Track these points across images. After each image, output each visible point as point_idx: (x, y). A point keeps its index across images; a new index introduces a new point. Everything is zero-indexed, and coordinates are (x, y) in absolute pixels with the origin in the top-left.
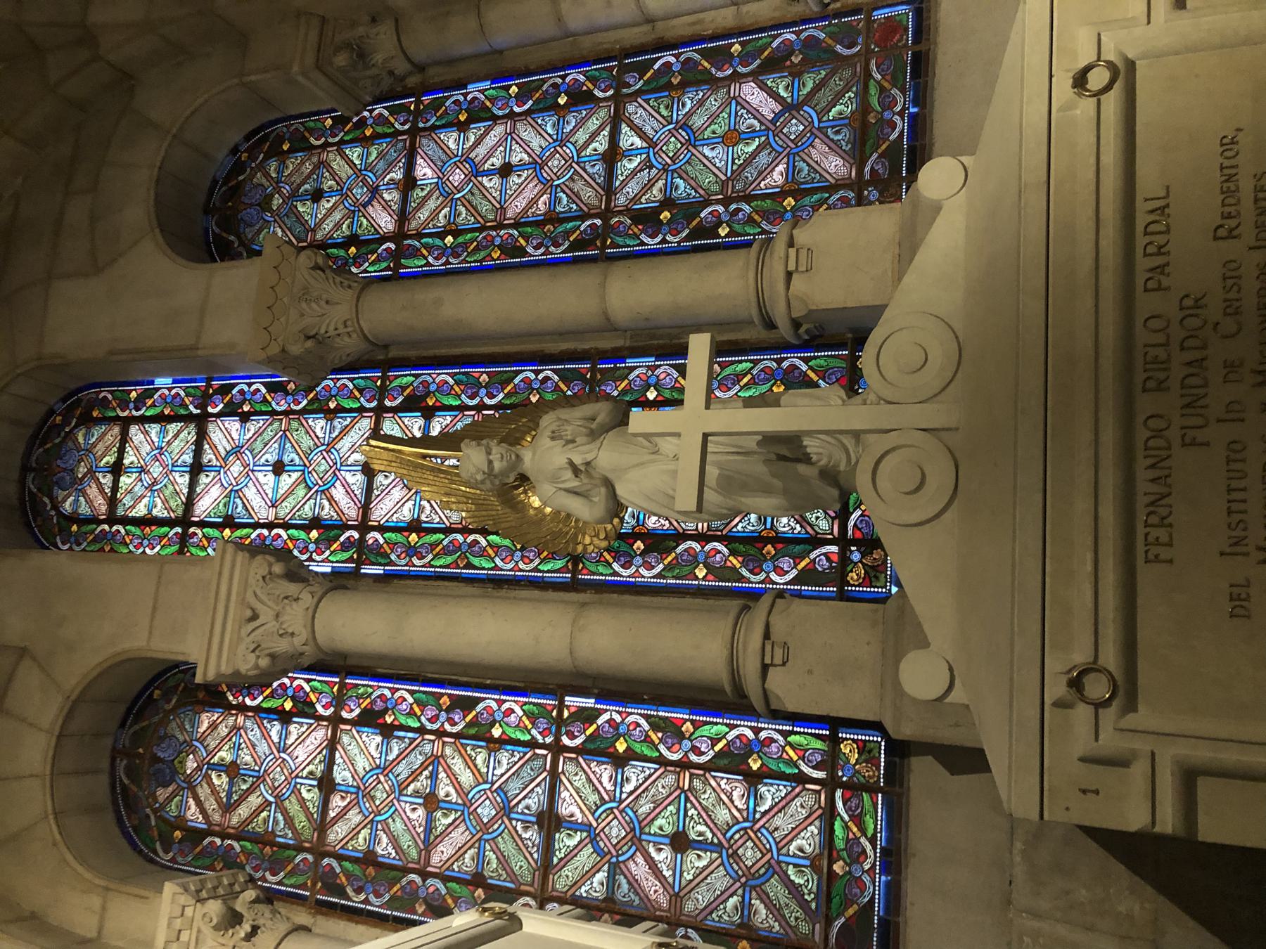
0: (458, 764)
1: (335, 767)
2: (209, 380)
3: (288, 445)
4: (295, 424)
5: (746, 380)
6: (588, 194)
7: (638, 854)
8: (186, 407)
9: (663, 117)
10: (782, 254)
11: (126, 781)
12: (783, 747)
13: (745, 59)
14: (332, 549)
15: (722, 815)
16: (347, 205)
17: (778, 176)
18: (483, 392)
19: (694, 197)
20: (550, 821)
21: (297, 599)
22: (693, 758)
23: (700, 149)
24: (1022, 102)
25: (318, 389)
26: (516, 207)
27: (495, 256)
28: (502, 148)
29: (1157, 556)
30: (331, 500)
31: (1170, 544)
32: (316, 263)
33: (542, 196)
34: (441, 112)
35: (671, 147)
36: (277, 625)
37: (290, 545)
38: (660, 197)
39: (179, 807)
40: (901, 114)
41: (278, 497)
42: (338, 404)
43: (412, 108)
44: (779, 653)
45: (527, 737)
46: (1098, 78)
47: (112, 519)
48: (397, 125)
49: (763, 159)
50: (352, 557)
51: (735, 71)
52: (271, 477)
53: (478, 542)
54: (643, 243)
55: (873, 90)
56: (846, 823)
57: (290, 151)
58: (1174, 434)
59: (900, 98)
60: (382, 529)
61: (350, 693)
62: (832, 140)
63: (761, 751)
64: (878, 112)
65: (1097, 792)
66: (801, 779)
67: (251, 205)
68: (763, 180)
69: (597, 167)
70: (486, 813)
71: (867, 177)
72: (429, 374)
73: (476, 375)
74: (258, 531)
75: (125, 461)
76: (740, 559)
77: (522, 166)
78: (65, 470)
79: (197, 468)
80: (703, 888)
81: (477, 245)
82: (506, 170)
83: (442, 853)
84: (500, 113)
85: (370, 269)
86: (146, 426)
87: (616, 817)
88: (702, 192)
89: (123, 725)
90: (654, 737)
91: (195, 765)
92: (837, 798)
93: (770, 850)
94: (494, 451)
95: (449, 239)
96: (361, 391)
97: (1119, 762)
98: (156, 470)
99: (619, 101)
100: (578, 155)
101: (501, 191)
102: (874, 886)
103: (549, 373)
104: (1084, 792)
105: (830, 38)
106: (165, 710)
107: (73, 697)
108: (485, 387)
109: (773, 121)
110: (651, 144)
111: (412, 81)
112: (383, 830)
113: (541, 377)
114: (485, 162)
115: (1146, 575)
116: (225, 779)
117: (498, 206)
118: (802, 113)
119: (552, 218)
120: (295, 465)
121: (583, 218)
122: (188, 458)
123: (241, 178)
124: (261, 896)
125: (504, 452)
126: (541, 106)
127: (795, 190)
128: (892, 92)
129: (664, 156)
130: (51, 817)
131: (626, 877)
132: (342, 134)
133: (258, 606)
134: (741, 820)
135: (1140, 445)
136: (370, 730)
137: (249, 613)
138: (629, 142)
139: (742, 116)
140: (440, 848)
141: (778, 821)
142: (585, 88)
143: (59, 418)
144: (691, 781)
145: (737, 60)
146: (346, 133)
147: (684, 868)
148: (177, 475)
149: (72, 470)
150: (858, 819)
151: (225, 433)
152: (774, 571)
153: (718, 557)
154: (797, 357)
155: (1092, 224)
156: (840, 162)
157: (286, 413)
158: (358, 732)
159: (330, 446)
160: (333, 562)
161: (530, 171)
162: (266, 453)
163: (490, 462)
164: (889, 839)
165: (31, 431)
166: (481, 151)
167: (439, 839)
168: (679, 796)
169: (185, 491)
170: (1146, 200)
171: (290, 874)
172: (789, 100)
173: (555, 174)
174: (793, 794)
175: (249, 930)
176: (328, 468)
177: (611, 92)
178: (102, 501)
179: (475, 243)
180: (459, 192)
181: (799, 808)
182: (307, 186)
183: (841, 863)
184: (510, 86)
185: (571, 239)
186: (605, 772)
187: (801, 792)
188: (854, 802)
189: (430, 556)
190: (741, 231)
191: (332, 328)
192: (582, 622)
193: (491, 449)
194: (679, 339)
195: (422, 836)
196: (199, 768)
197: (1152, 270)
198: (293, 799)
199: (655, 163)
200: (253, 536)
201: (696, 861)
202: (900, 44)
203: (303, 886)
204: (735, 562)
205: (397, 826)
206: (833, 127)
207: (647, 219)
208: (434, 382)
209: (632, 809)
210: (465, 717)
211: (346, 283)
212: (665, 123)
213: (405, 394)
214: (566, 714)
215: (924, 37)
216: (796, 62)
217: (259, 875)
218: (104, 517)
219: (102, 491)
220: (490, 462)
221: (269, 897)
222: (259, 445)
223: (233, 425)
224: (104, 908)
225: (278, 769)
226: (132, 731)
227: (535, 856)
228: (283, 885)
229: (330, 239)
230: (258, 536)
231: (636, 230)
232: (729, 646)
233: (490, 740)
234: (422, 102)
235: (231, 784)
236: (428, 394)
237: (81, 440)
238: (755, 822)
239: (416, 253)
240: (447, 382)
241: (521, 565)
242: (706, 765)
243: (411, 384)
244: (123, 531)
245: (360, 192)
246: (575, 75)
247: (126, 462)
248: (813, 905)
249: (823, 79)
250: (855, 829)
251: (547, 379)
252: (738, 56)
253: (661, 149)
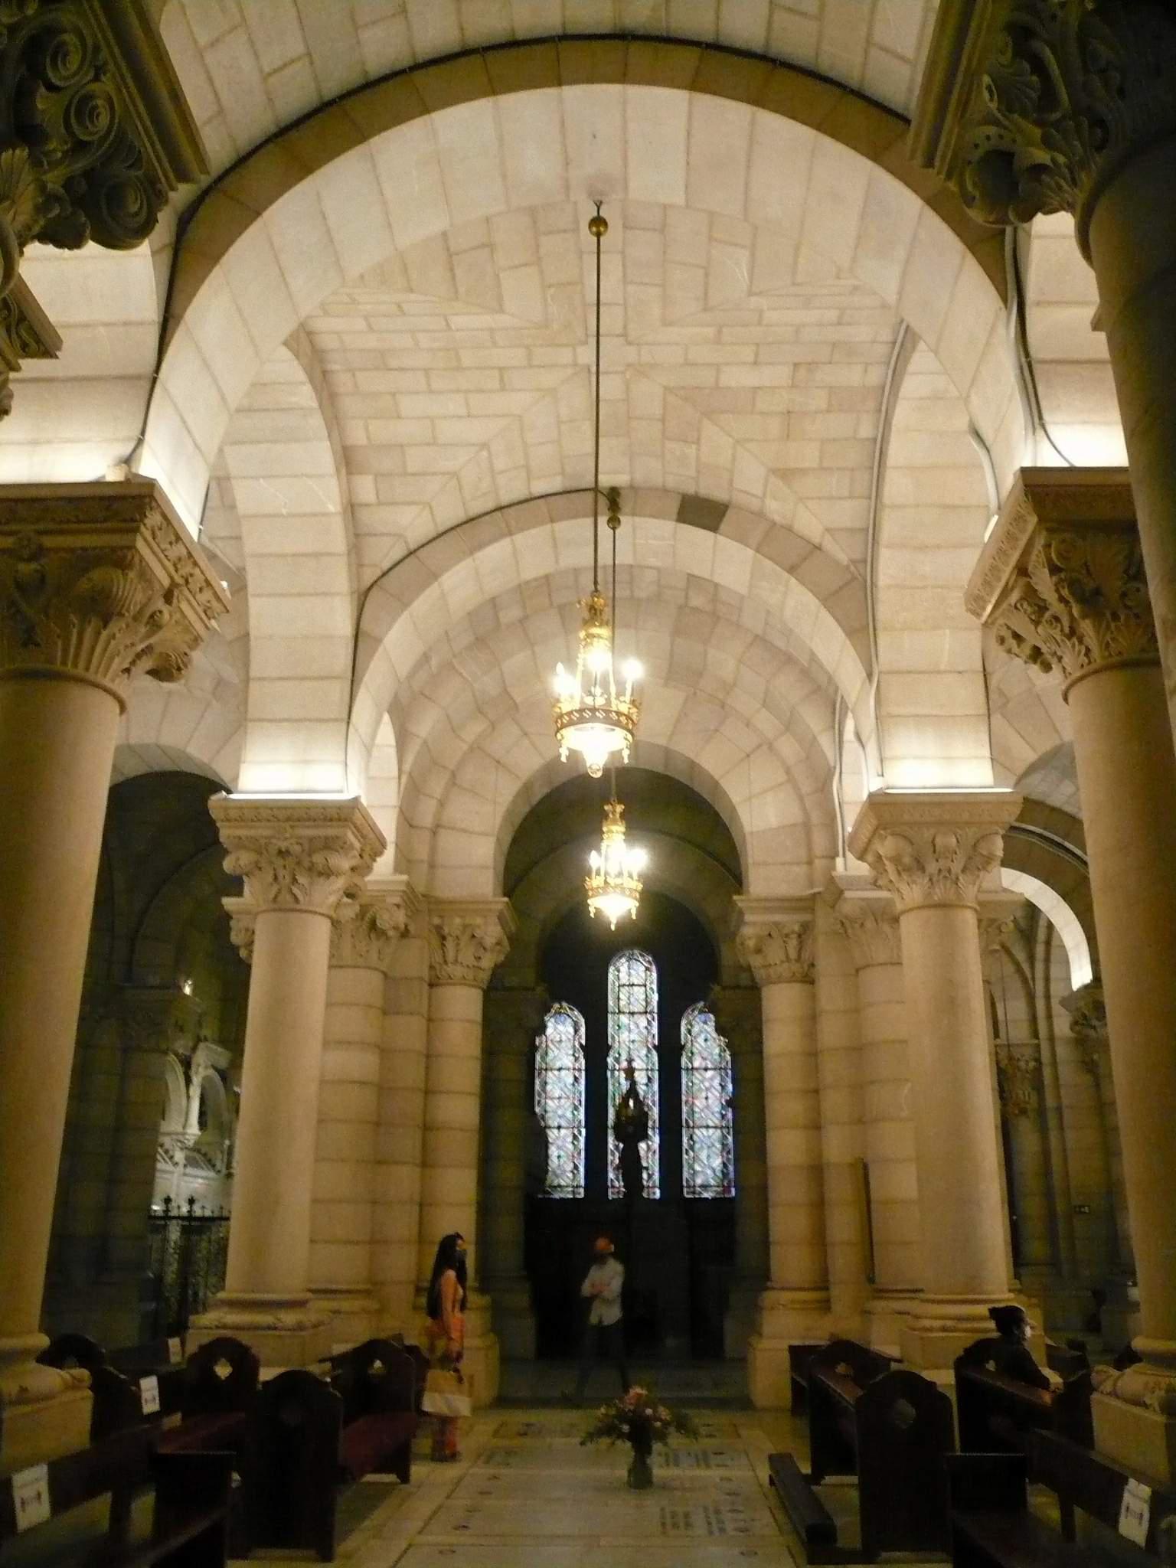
26: (697, 1102)
99: (722, 1128)
119: (693, 1112)
166: (713, 1090)
207: (691, 1138)
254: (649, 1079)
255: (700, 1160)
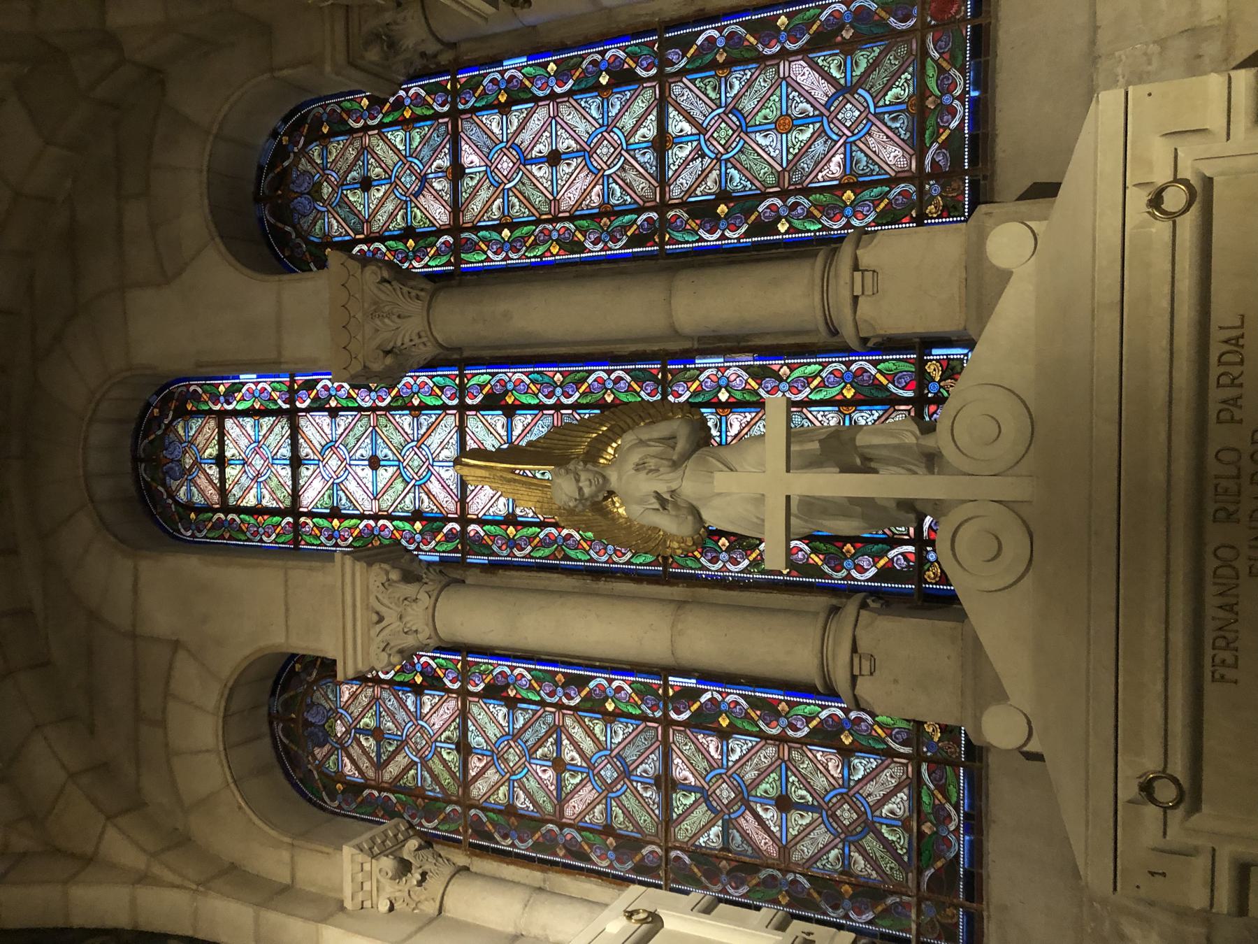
0: (578, 733)
1: (470, 734)
2: (292, 376)
3: (380, 441)
4: (383, 421)
5: (816, 382)
6: (641, 185)
7: (747, 812)
8: (275, 402)
9: (710, 99)
10: (848, 280)
11: (286, 741)
12: (872, 726)
13: (793, 34)
14: (437, 539)
15: (820, 782)
16: (398, 194)
17: (835, 167)
18: (559, 391)
19: (750, 190)
20: (666, 783)
21: (416, 600)
22: (790, 733)
23: (753, 136)
24: (1095, 214)
25: (399, 386)
26: (569, 198)
27: (555, 251)
28: (547, 134)
29: (1223, 661)
30: (429, 493)
31: (1235, 666)
32: (382, 277)
33: (594, 187)
34: (479, 91)
35: (723, 133)
36: (402, 625)
37: (397, 535)
38: (715, 189)
39: (336, 763)
40: (961, 98)
41: (379, 490)
42: (421, 401)
43: (449, 87)
44: (866, 665)
45: (638, 712)
46: (1175, 199)
47: (226, 509)
48: (435, 106)
49: (819, 147)
50: (457, 547)
51: (783, 48)
52: (368, 471)
53: (572, 536)
54: (701, 239)
55: (931, 71)
56: (932, 792)
57: (333, 134)
58: (1242, 565)
59: (960, 81)
60: (481, 522)
61: (473, 669)
62: (889, 128)
63: (851, 728)
64: (936, 97)
65: (1164, 874)
66: (890, 754)
67: (301, 194)
68: (821, 171)
69: (647, 156)
70: (609, 774)
71: (928, 169)
72: (505, 373)
73: (551, 374)
74: (365, 522)
75: (227, 454)
76: (821, 556)
77: (571, 154)
78: (172, 461)
79: (296, 462)
80: (807, 842)
81: (535, 239)
82: (554, 158)
83: (574, 808)
84: (540, 94)
85: (431, 263)
86: (241, 420)
87: (725, 781)
88: (758, 184)
89: (273, 694)
90: (753, 714)
91: (344, 729)
92: (923, 770)
93: (866, 813)
94: (583, 478)
95: (506, 233)
96: (442, 389)
97: (1188, 853)
98: (258, 463)
99: (663, 80)
100: (626, 142)
101: (552, 181)
102: (959, 844)
103: (621, 374)
104: (1153, 874)
105: (883, 9)
106: (308, 682)
107: (230, 684)
108: (560, 386)
109: (827, 106)
110: (702, 130)
111: (446, 58)
112: (520, 787)
113: (613, 376)
114: (532, 149)
115: (1212, 691)
116: (372, 741)
117: (551, 198)
118: (856, 96)
119: (607, 211)
120: (389, 460)
121: (639, 211)
122: (286, 451)
123: (286, 164)
124: (423, 843)
125: (591, 478)
126: (583, 86)
127: (854, 183)
128: (951, 72)
129: (715, 143)
130: (232, 785)
131: (738, 831)
132: (381, 116)
133: (383, 610)
134: (837, 786)
135: (1209, 572)
136: (496, 702)
137: (375, 618)
138: (678, 128)
139: (793, 99)
140: (572, 803)
141: (870, 788)
142: (626, 66)
143: (156, 411)
144: (789, 753)
145: (784, 34)
146: (385, 115)
147: (789, 824)
148: (279, 468)
149: (180, 461)
150: (943, 789)
151: (316, 428)
152: (855, 568)
153: (800, 555)
154: (865, 360)
155: (1166, 355)
156: (899, 153)
157: (374, 409)
158: (485, 704)
159: (420, 442)
160: (439, 552)
161: (579, 160)
162: (359, 448)
163: (580, 489)
164: (971, 806)
165: (133, 426)
166: (526, 137)
167: (570, 796)
168: (780, 765)
169: (290, 483)
170: (1221, 328)
171: (443, 821)
172: (842, 82)
173: (605, 163)
174: (884, 766)
175: (420, 878)
176: (421, 464)
177: (654, 71)
178: (212, 491)
179: (533, 238)
180: (510, 182)
181: (890, 777)
182: (354, 174)
183: (929, 824)
184: (548, 63)
185: (629, 234)
186: (712, 744)
187: (890, 764)
188: (937, 775)
189: (529, 548)
190: (800, 227)
191: (407, 340)
192: (680, 626)
193: (579, 476)
194: (748, 341)
195: (555, 793)
196: (348, 732)
197: (1224, 402)
198: (436, 759)
199: (706, 151)
200: (361, 526)
201: (799, 820)
202: (958, 17)
203: (457, 832)
204: (816, 559)
205: (532, 785)
206: (890, 113)
207: (703, 212)
208: (510, 381)
209: (738, 775)
210: (579, 693)
211: (414, 293)
212: (714, 107)
213: (484, 392)
214: (671, 692)
215: (984, 8)
216: (848, 37)
217: (416, 821)
218: (217, 506)
219: (211, 482)
220: (580, 489)
221: (429, 841)
222: (351, 441)
223: (323, 419)
224: (292, 857)
225: (419, 734)
226: (282, 699)
227: (657, 812)
228: (438, 830)
229: (386, 231)
230: (366, 526)
231: (694, 225)
232: (820, 655)
233: (605, 713)
234: (458, 80)
235: (379, 746)
236: (506, 392)
237: (181, 432)
238: (850, 788)
239: (474, 248)
240: (523, 381)
241: (615, 559)
242: (803, 740)
243: (489, 382)
244: (237, 519)
245: (408, 180)
246: (613, 51)
247: (228, 454)
248: (906, 859)
249: (877, 57)
250: (940, 796)
251: (620, 379)
252: (785, 30)
253: (712, 135)
254: (493, 402)
255: (794, 164)
